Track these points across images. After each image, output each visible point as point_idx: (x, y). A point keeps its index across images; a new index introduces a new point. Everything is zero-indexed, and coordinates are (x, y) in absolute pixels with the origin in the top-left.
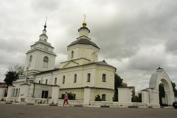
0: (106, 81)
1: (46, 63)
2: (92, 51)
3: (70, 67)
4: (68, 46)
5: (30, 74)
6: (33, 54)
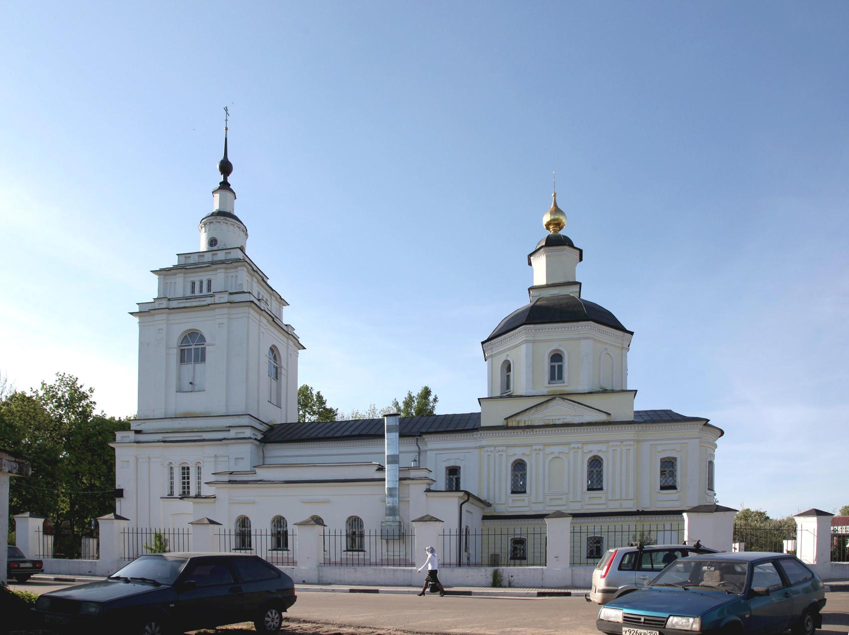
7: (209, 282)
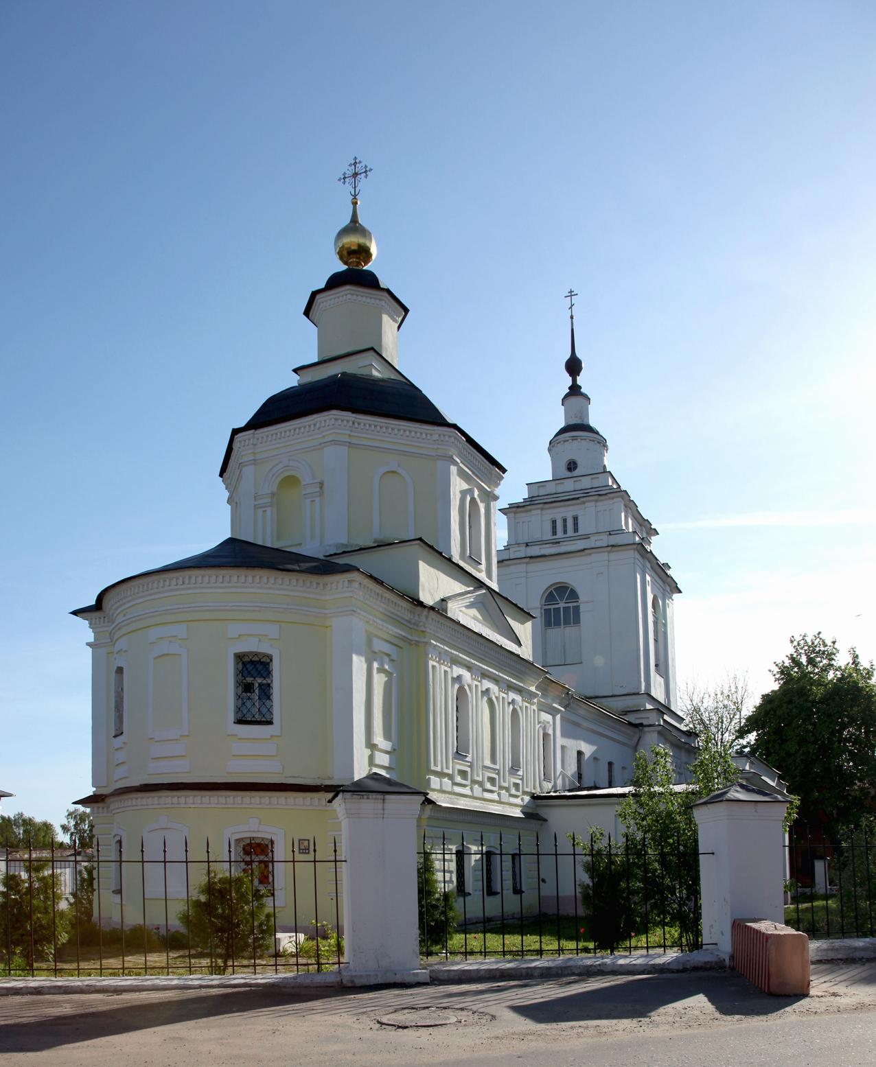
7: (575, 519)
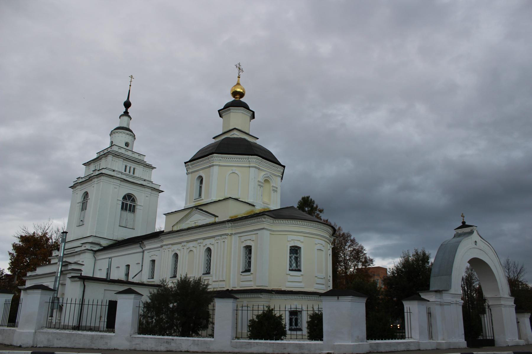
0: (302, 270)
1: (127, 215)
2: (261, 176)
3: (194, 225)
4: (185, 163)
5: (83, 248)
6: (87, 188)
7: (134, 169)
